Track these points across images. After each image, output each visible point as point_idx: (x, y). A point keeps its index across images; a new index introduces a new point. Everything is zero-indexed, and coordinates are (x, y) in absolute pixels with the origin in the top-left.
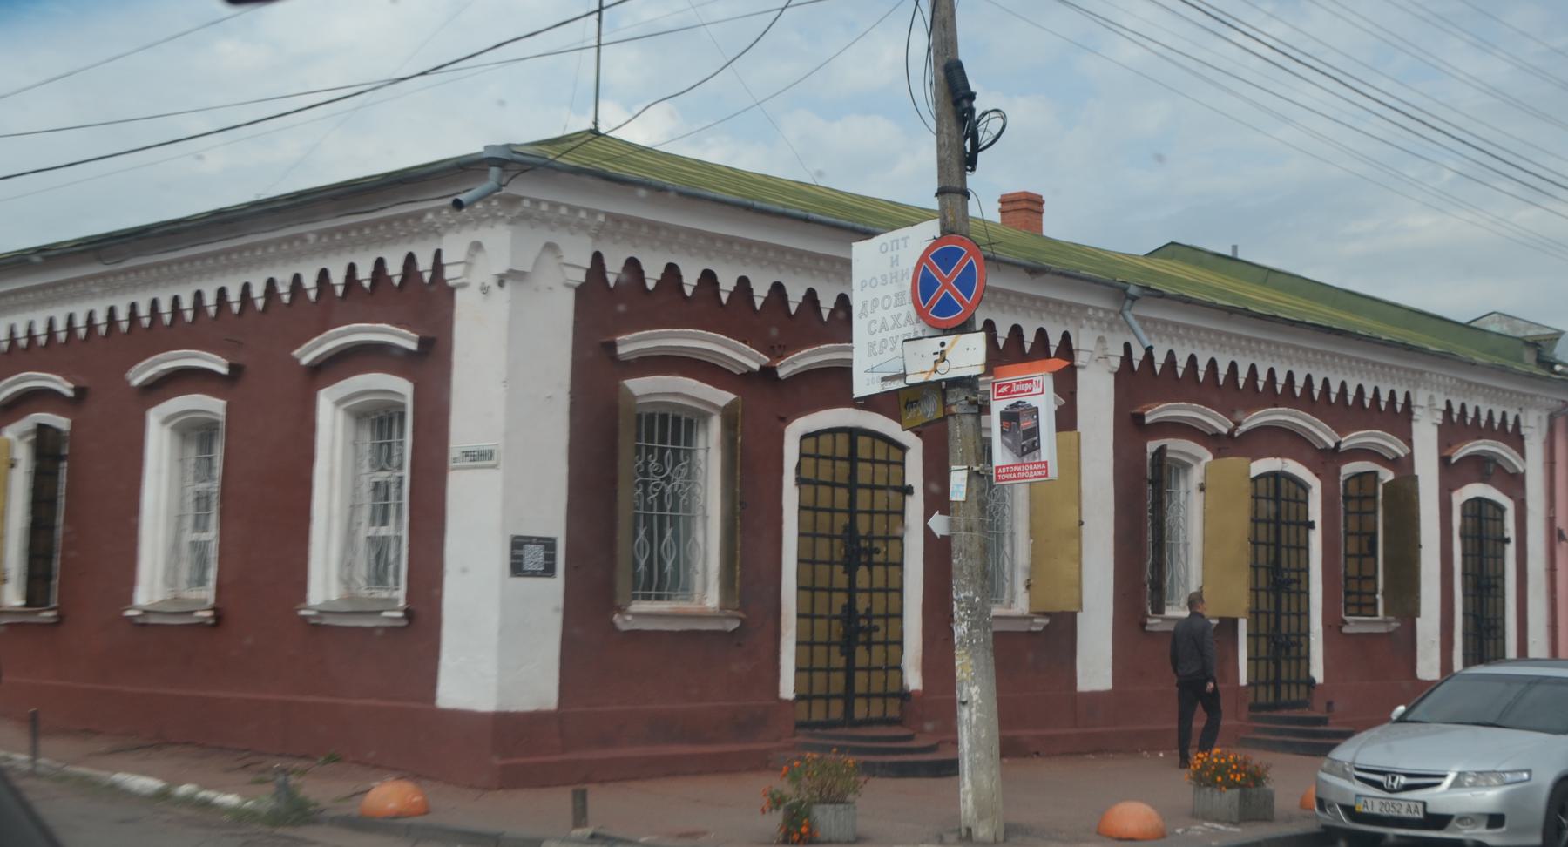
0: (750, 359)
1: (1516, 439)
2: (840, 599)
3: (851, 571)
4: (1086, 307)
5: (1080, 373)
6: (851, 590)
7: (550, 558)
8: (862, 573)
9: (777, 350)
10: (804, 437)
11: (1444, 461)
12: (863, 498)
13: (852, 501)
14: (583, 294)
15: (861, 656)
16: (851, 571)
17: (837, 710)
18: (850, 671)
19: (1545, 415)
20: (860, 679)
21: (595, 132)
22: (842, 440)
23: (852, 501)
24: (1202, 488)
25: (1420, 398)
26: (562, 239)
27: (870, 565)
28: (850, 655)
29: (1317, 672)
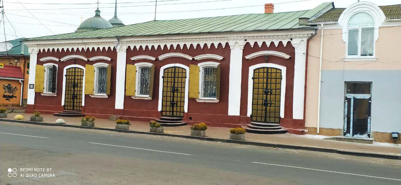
0: (57, 60)
1: (290, 49)
2: (72, 92)
3: (74, 88)
4: (114, 42)
5: (118, 54)
6: (74, 91)
7: (33, 86)
8: (76, 88)
9: (60, 58)
10: (67, 69)
11: (244, 60)
12: (76, 77)
13: (75, 78)
14: (38, 54)
15: (75, 100)
16: (74, 88)
17: (72, 108)
18: (74, 102)
19: (305, 40)
20: (75, 104)
21: (155, 20)
22: (74, 69)
23: (75, 78)
24: (200, 71)
25: (231, 43)
26: (34, 48)
27: (77, 87)
28: (74, 101)
29: (186, 110)
